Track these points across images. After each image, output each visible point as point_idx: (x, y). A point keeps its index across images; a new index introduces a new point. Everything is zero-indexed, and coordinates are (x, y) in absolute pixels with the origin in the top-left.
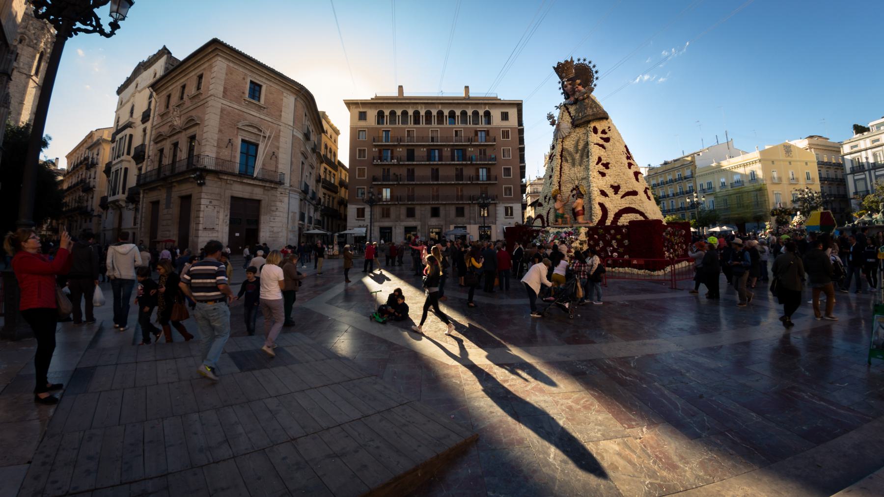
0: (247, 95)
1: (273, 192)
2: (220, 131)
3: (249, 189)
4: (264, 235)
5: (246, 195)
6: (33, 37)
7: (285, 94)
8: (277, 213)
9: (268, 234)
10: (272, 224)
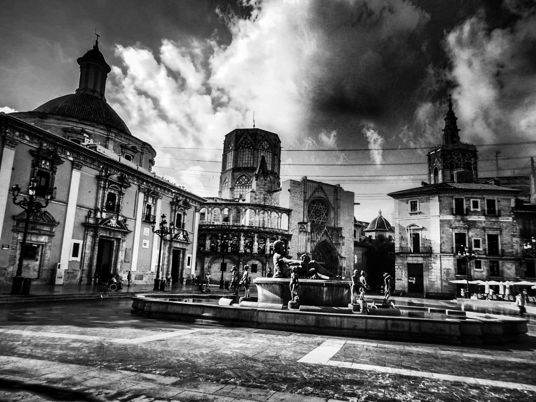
0: (410, 212)
1: (430, 258)
2: (400, 233)
3: (415, 258)
4: (426, 282)
5: (415, 262)
6: (457, 161)
7: (431, 198)
8: (433, 270)
9: (428, 283)
10: (430, 277)
